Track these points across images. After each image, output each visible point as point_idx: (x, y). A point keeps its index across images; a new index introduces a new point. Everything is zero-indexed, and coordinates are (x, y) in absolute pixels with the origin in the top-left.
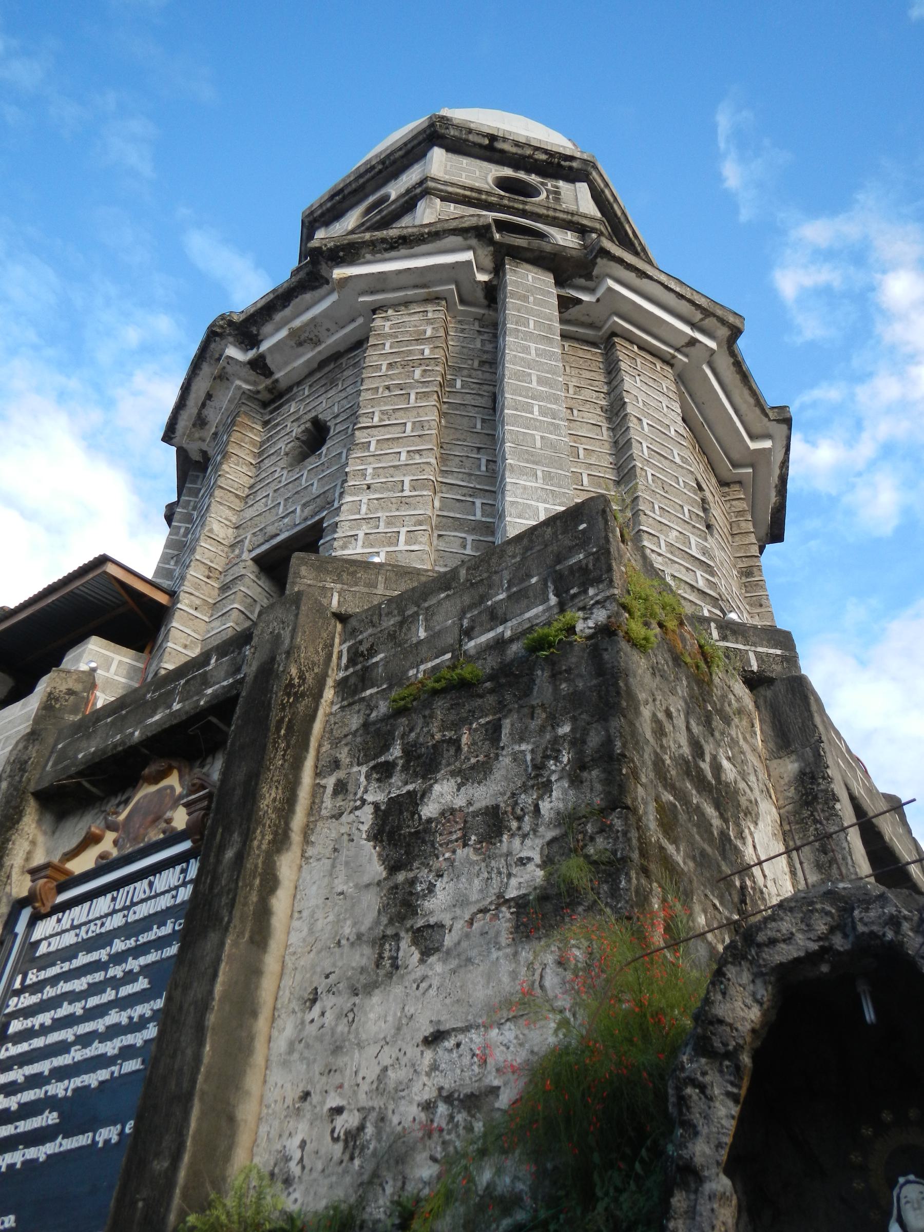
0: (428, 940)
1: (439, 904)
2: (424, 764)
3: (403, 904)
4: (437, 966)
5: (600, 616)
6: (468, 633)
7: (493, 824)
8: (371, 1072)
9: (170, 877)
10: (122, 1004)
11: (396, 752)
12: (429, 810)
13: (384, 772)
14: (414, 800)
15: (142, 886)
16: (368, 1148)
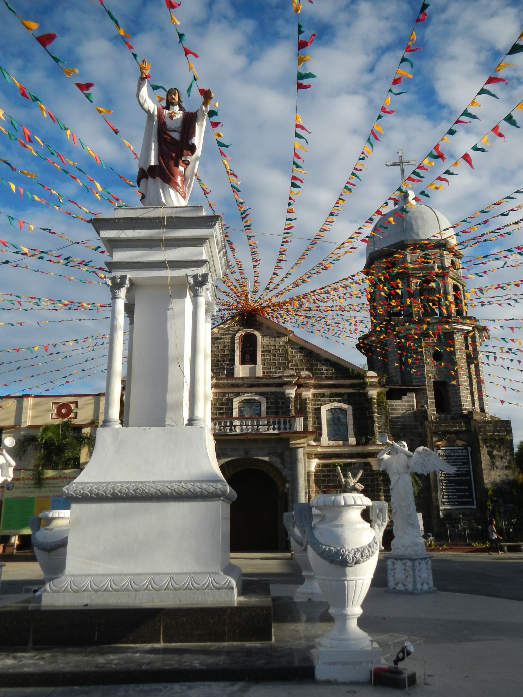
0: (497, 467)
1: (497, 464)
2: (493, 448)
3: (493, 464)
4: (498, 470)
5: (511, 438)
6: (494, 432)
7: (502, 458)
8: (493, 478)
9: (461, 451)
10: (460, 465)
11: (488, 445)
12: (494, 454)
13: (487, 447)
14: (492, 452)
15: (456, 451)
16: (494, 484)
